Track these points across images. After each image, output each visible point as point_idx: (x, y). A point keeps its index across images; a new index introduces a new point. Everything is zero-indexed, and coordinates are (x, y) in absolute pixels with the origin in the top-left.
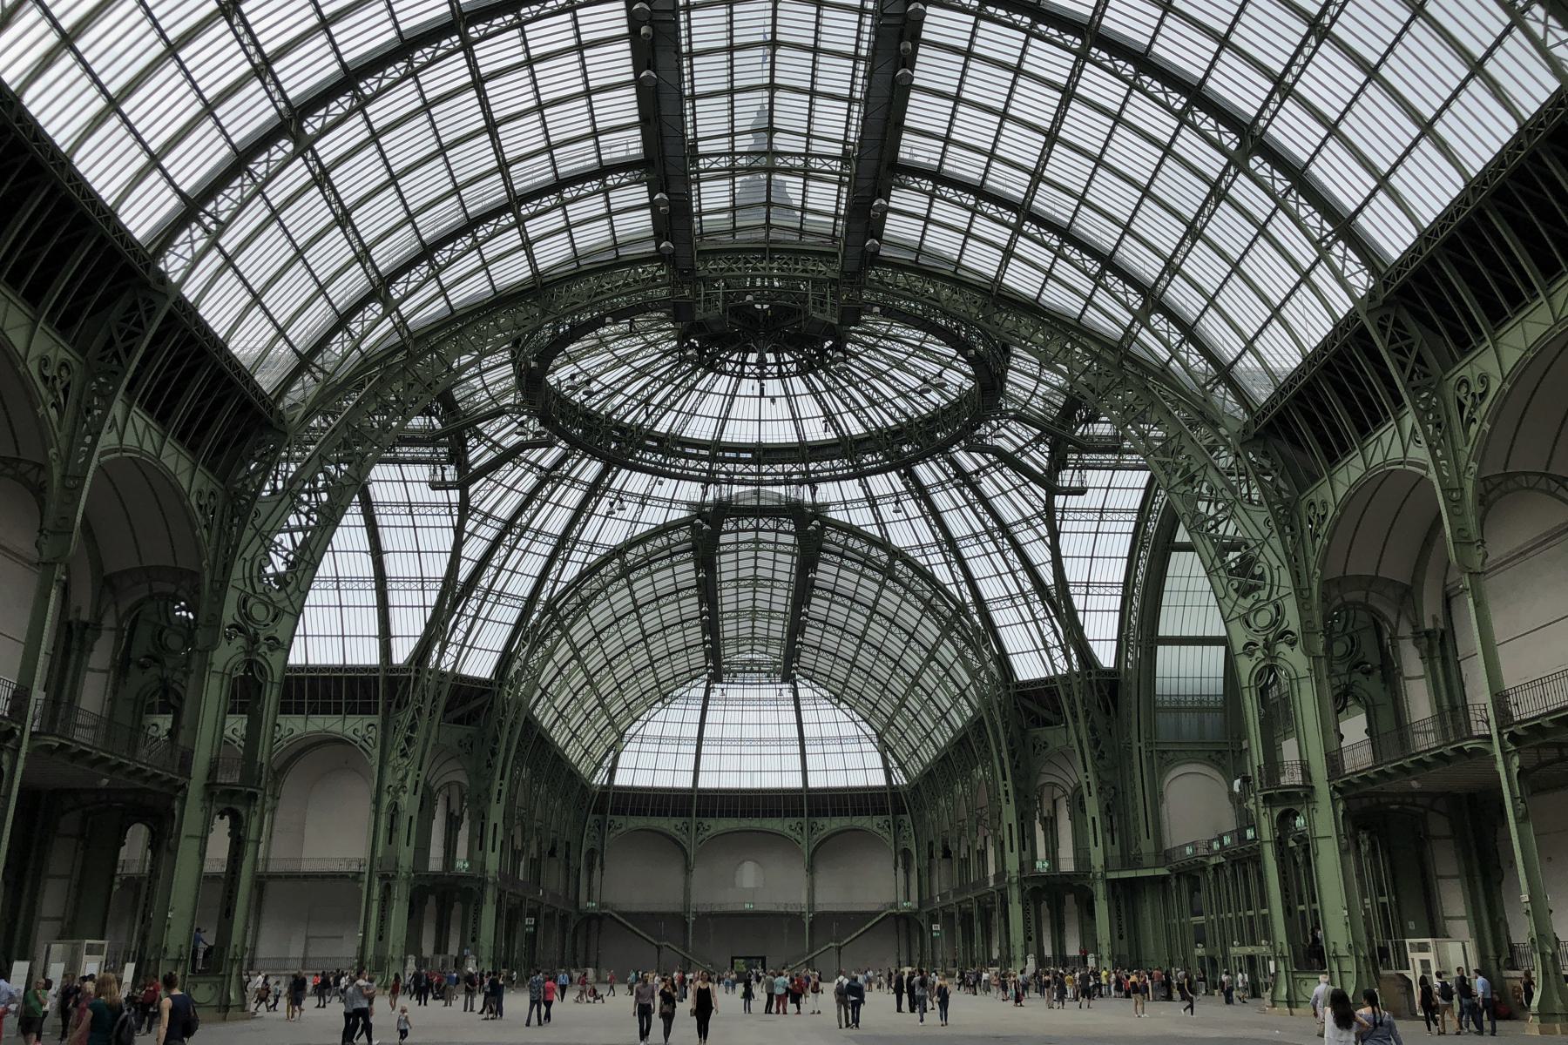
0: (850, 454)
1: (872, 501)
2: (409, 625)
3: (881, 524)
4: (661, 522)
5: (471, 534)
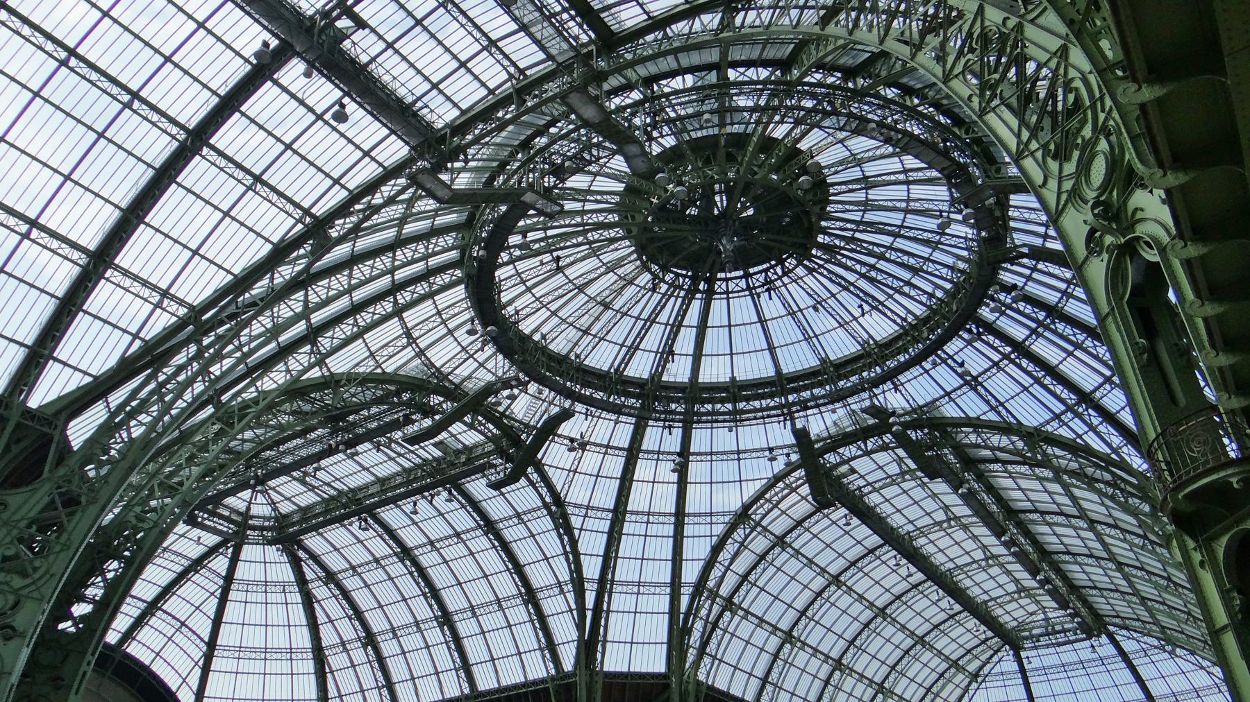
0: (922, 341)
1: (972, 382)
2: (565, 631)
3: (996, 405)
4: (770, 475)
5: (581, 530)
